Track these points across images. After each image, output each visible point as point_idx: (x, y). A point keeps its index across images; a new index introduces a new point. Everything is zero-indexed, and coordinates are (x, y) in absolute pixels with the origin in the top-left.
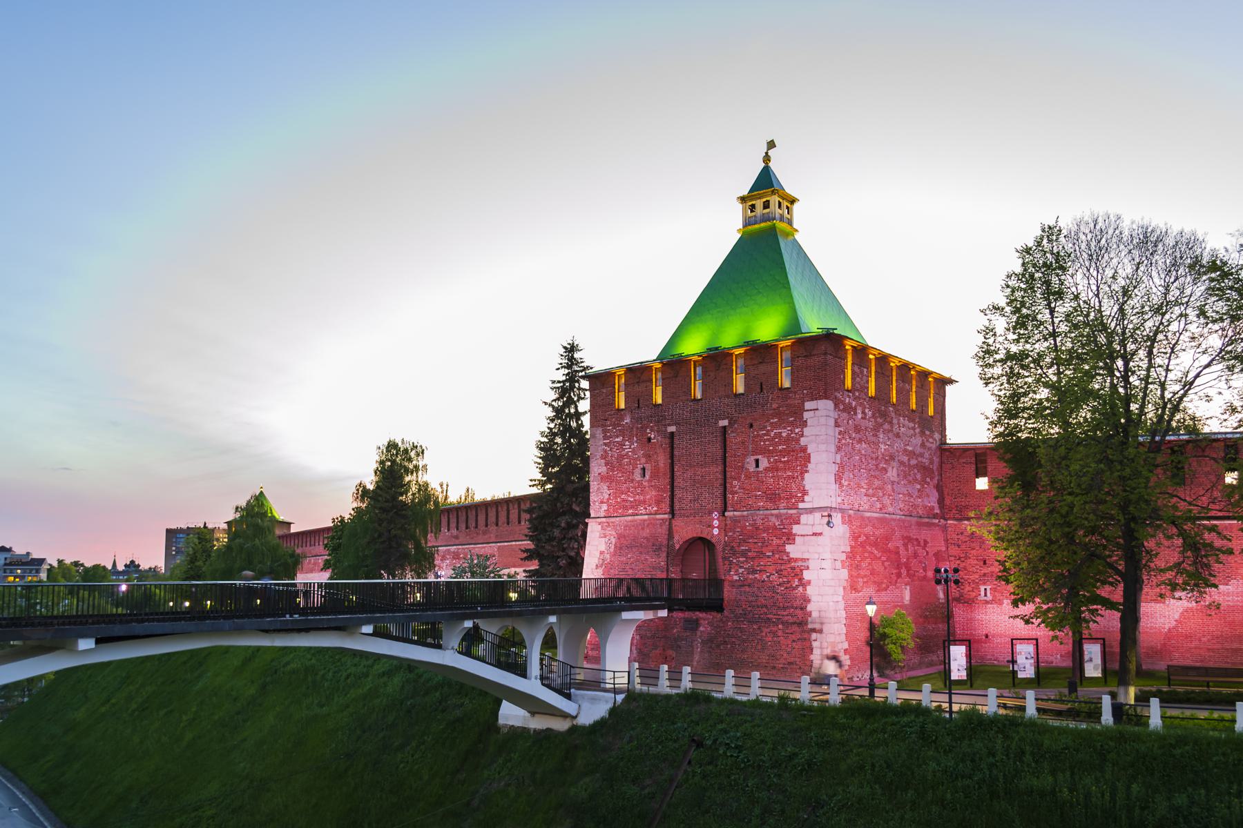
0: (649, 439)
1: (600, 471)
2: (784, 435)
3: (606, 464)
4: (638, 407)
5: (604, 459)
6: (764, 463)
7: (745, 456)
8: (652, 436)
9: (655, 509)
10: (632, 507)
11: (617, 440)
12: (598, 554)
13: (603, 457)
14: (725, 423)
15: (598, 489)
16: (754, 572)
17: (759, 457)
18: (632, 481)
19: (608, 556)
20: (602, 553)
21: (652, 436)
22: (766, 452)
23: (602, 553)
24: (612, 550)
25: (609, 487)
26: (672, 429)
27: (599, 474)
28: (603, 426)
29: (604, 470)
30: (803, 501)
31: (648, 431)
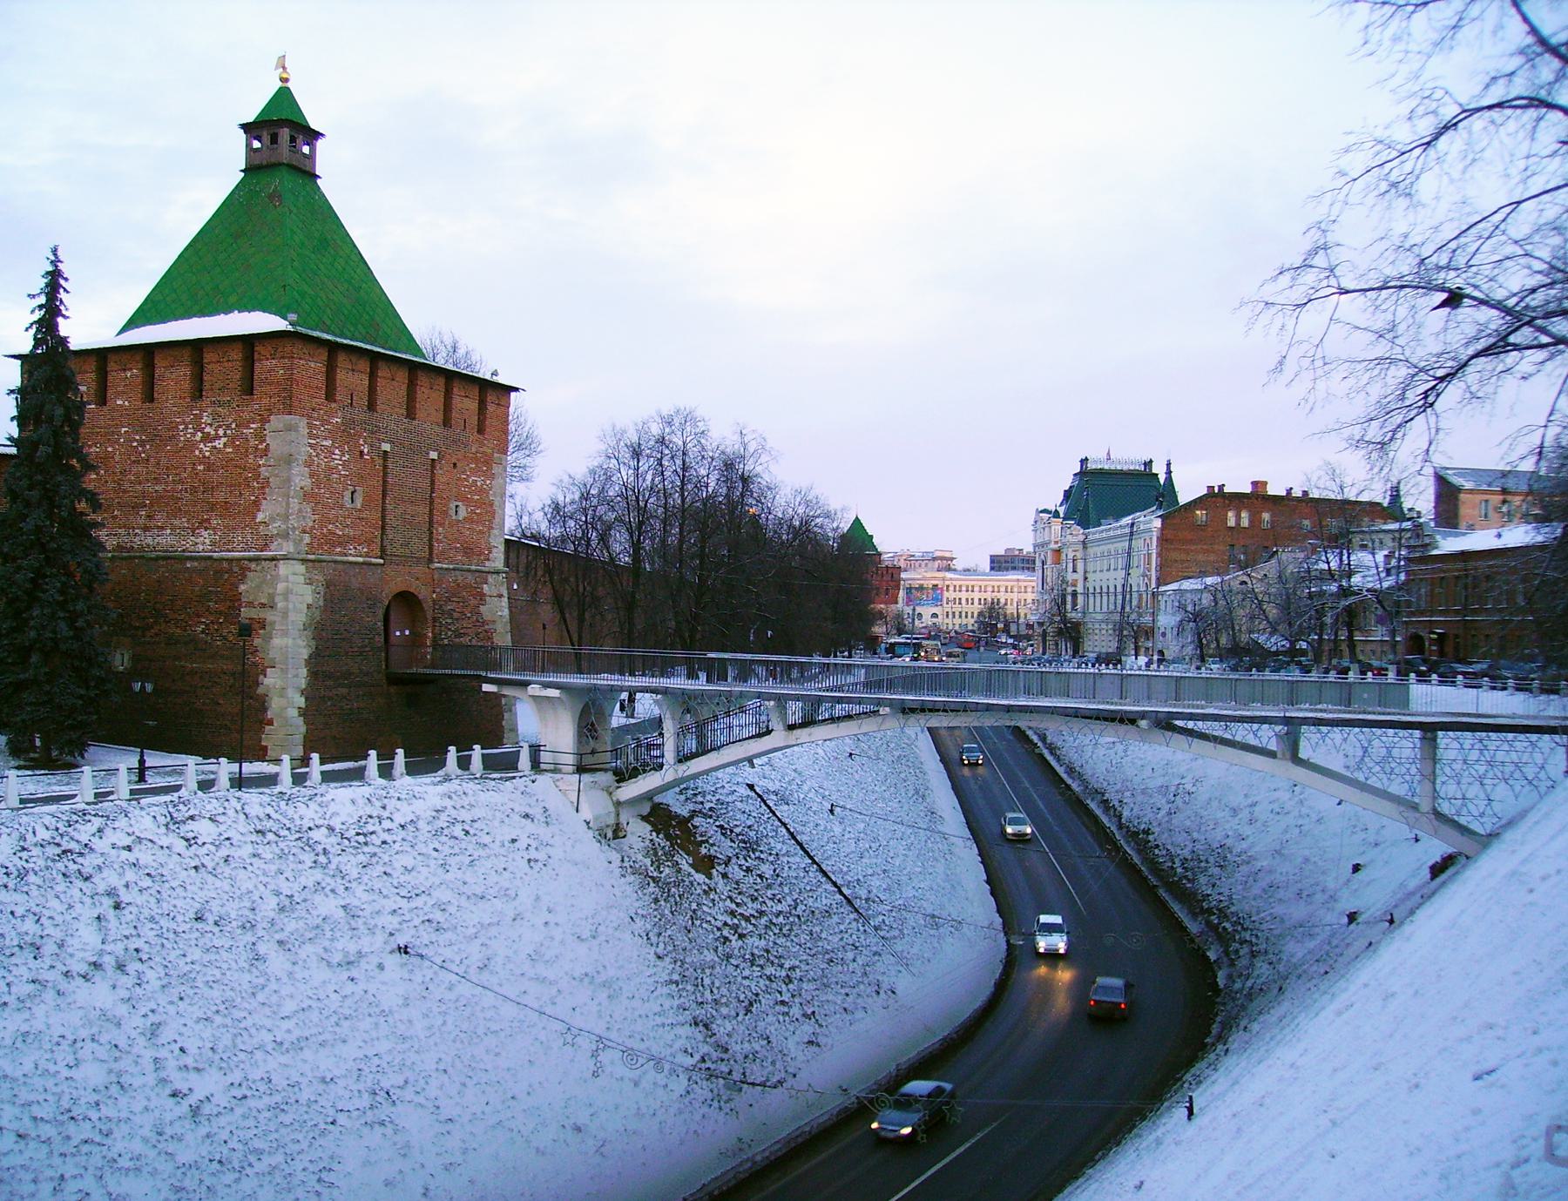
0: (362, 453)
1: (303, 484)
2: (479, 484)
3: (311, 476)
4: (351, 404)
5: (309, 466)
6: (463, 513)
7: (449, 499)
8: (366, 451)
9: (365, 550)
10: (340, 544)
11: (324, 443)
12: (305, 610)
13: (308, 464)
14: (434, 455)
15: (300, 511)
16: (460, 635)
17: (460, 504)
18: (342, 507)
19: (318, 613)
20: (309, 606)
21: (366, 451)
22: (465, 500)
23: (309, 606)
24: (321, 603)
25: (314, 510)
26: (386, 447)
27: (301, 488)
28: (310, 417)
29: (307, 482)
30: (488, 560)
31: (361, 442)
